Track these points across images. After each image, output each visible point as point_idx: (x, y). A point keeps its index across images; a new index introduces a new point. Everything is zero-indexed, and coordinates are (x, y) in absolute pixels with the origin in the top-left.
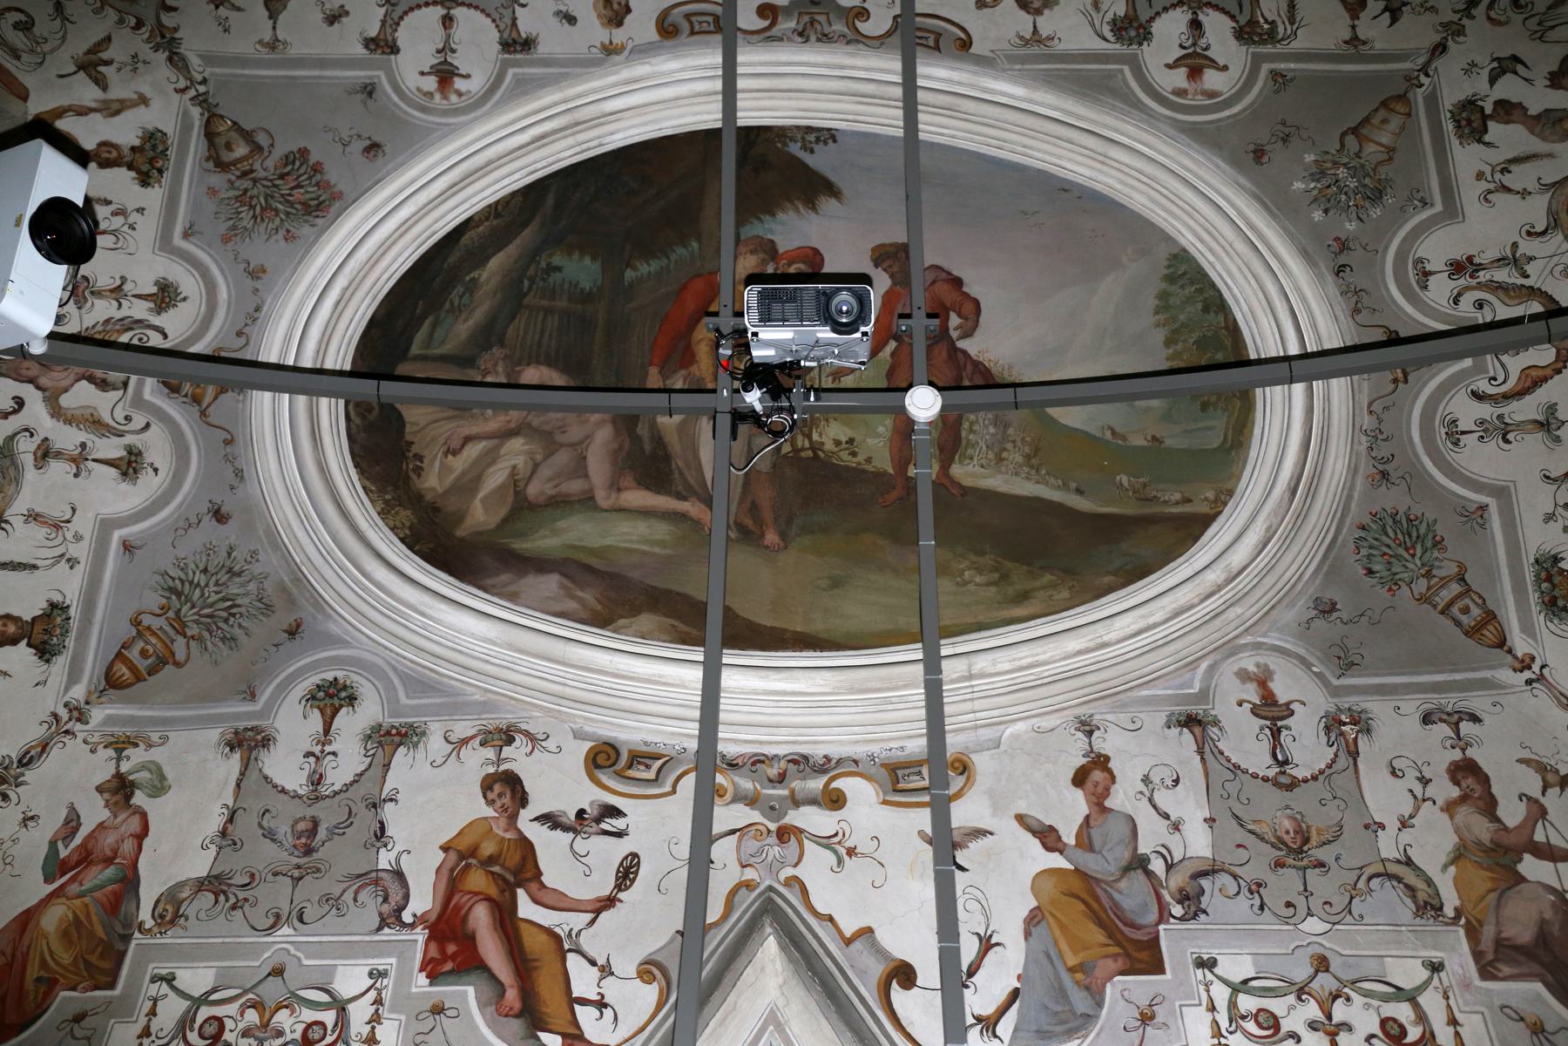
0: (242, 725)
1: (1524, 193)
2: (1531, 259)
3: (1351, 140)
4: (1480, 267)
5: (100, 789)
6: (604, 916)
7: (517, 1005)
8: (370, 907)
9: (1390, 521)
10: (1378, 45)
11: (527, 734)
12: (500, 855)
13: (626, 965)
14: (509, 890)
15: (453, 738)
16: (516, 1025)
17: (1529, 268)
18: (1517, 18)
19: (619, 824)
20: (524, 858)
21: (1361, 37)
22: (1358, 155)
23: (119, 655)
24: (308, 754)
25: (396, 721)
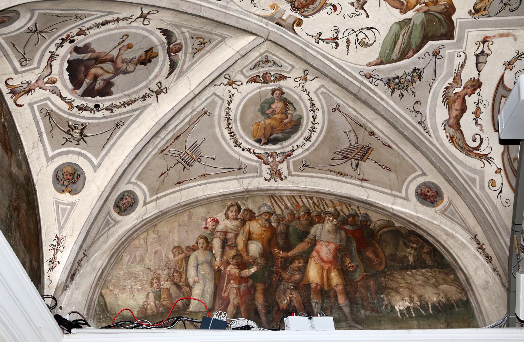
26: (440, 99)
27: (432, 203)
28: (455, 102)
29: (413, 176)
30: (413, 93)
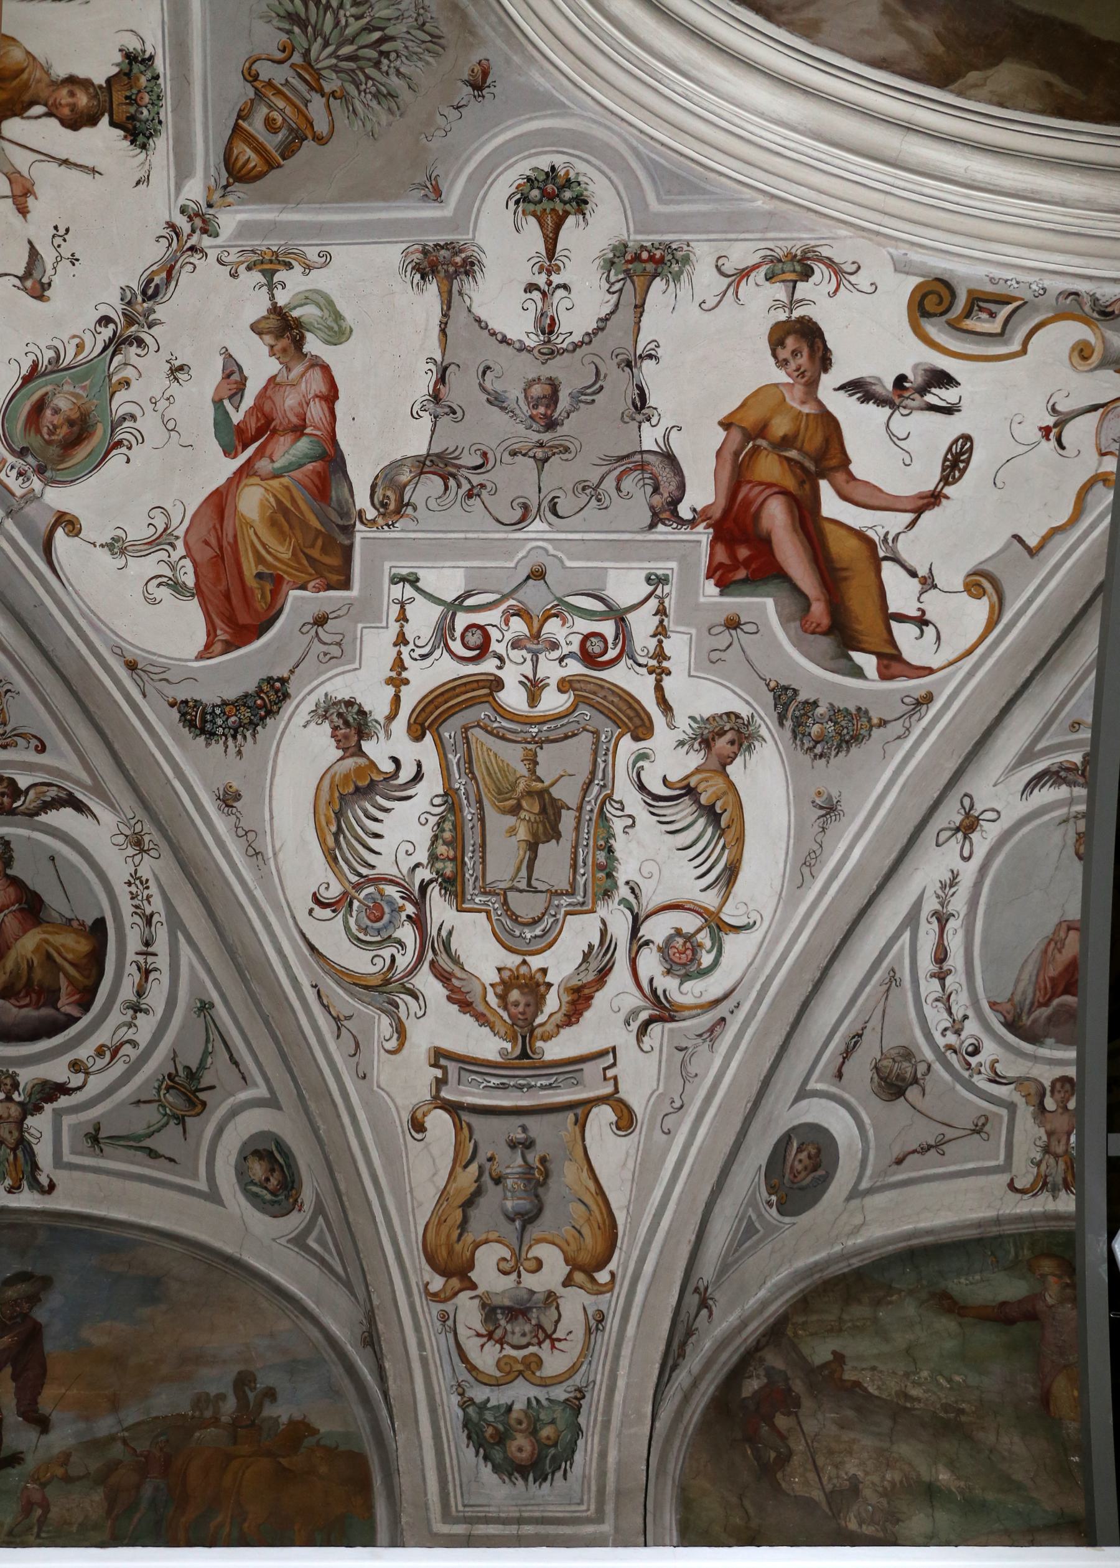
0: (431, 239)
5: (256, 328)
6: (927, 516)
7: (826, 622)
8: (637, 501)
11: (830, 263)
12: (796, 435)
13: (951, 577)
14: (809, 479)
15: (728, 268)
16: (825, 643)
19: (948, 395)
20: (827, 441)
23: (237, 128)
24: (531, 287)
25: (647, 239)
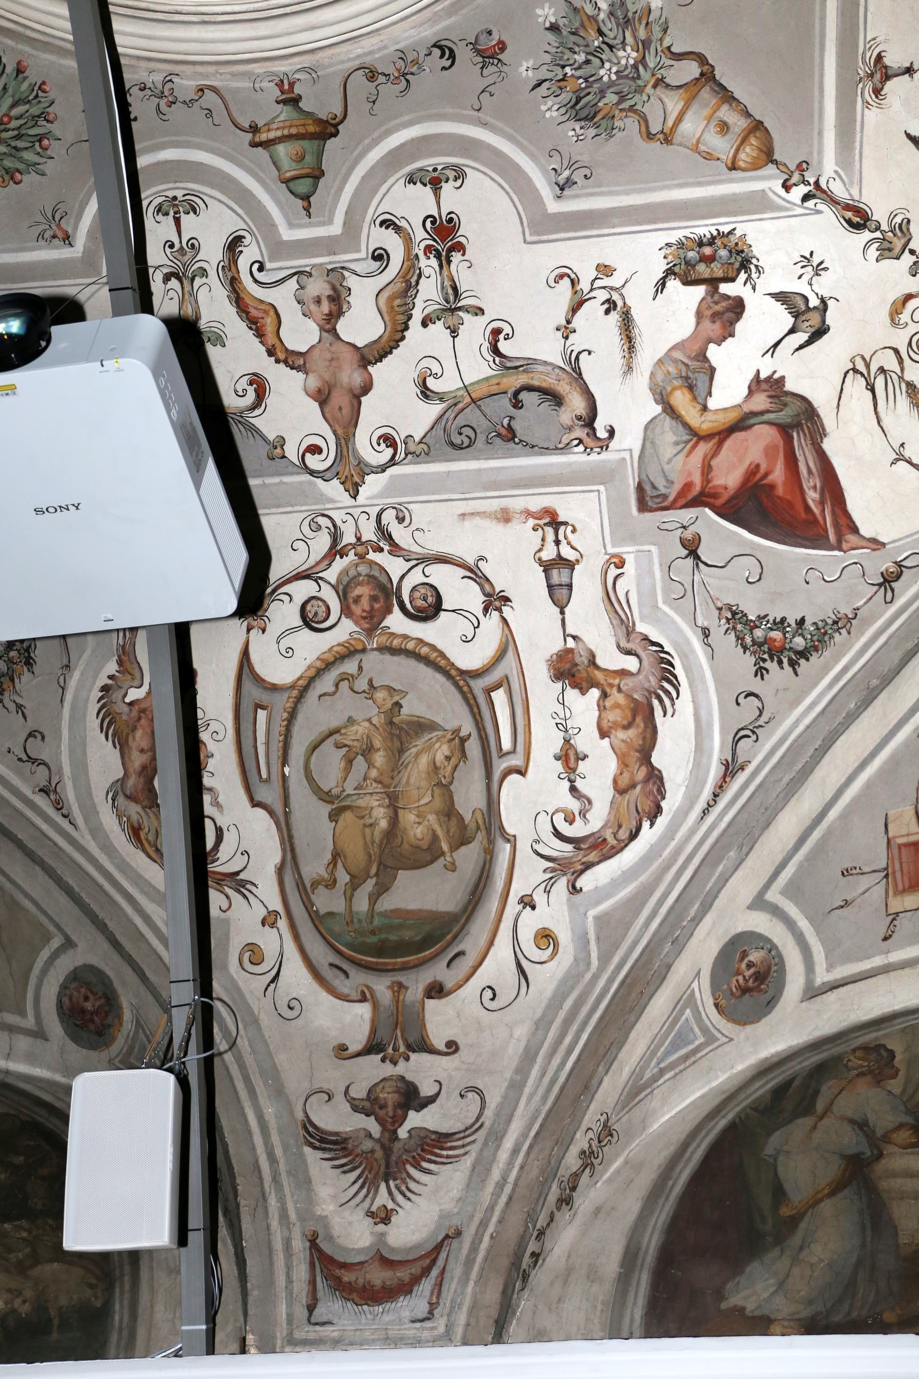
1: (567, 330)
2: (454, 332)
3: (692, 70)
4: (444, 260)
9: (35, 111)
10: (872, 117)
17: (438, 329)
18: (900, 340)
21: (889, 86)
22: (660, 82)
26: (93, 723)
27: (100, 1034)
28: (134, 729)
29: (45, 954)
30: (19, 707)
